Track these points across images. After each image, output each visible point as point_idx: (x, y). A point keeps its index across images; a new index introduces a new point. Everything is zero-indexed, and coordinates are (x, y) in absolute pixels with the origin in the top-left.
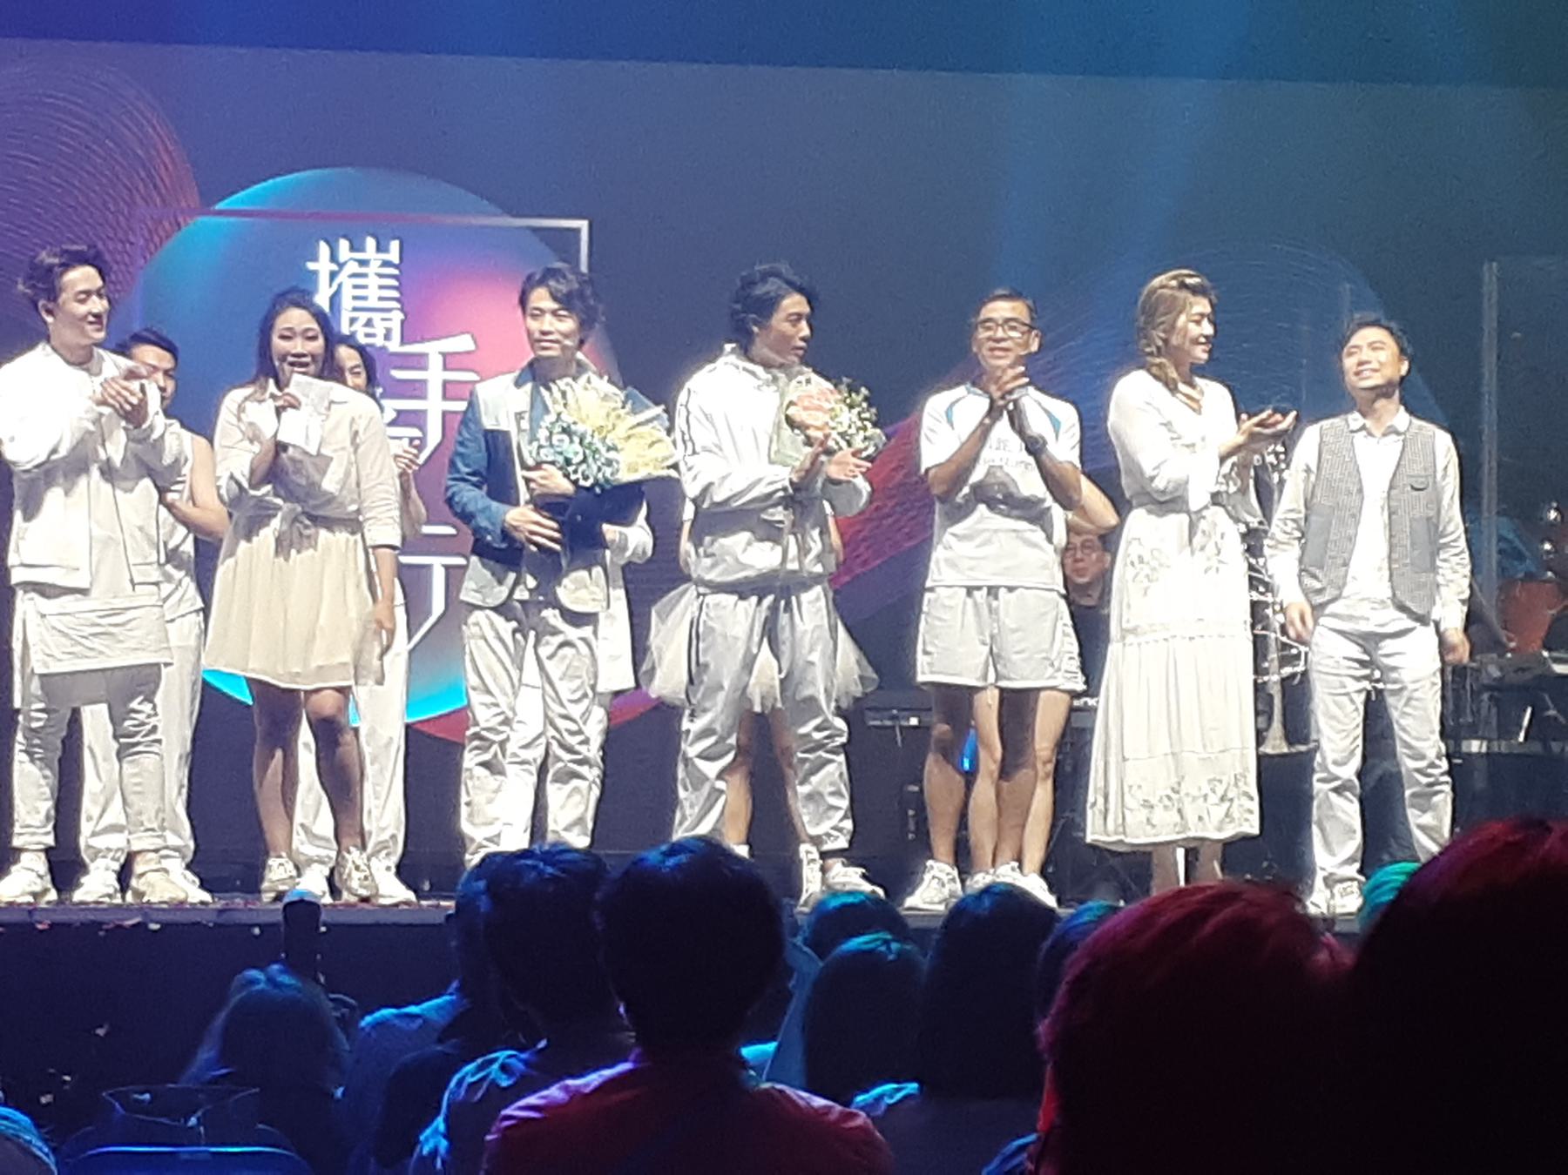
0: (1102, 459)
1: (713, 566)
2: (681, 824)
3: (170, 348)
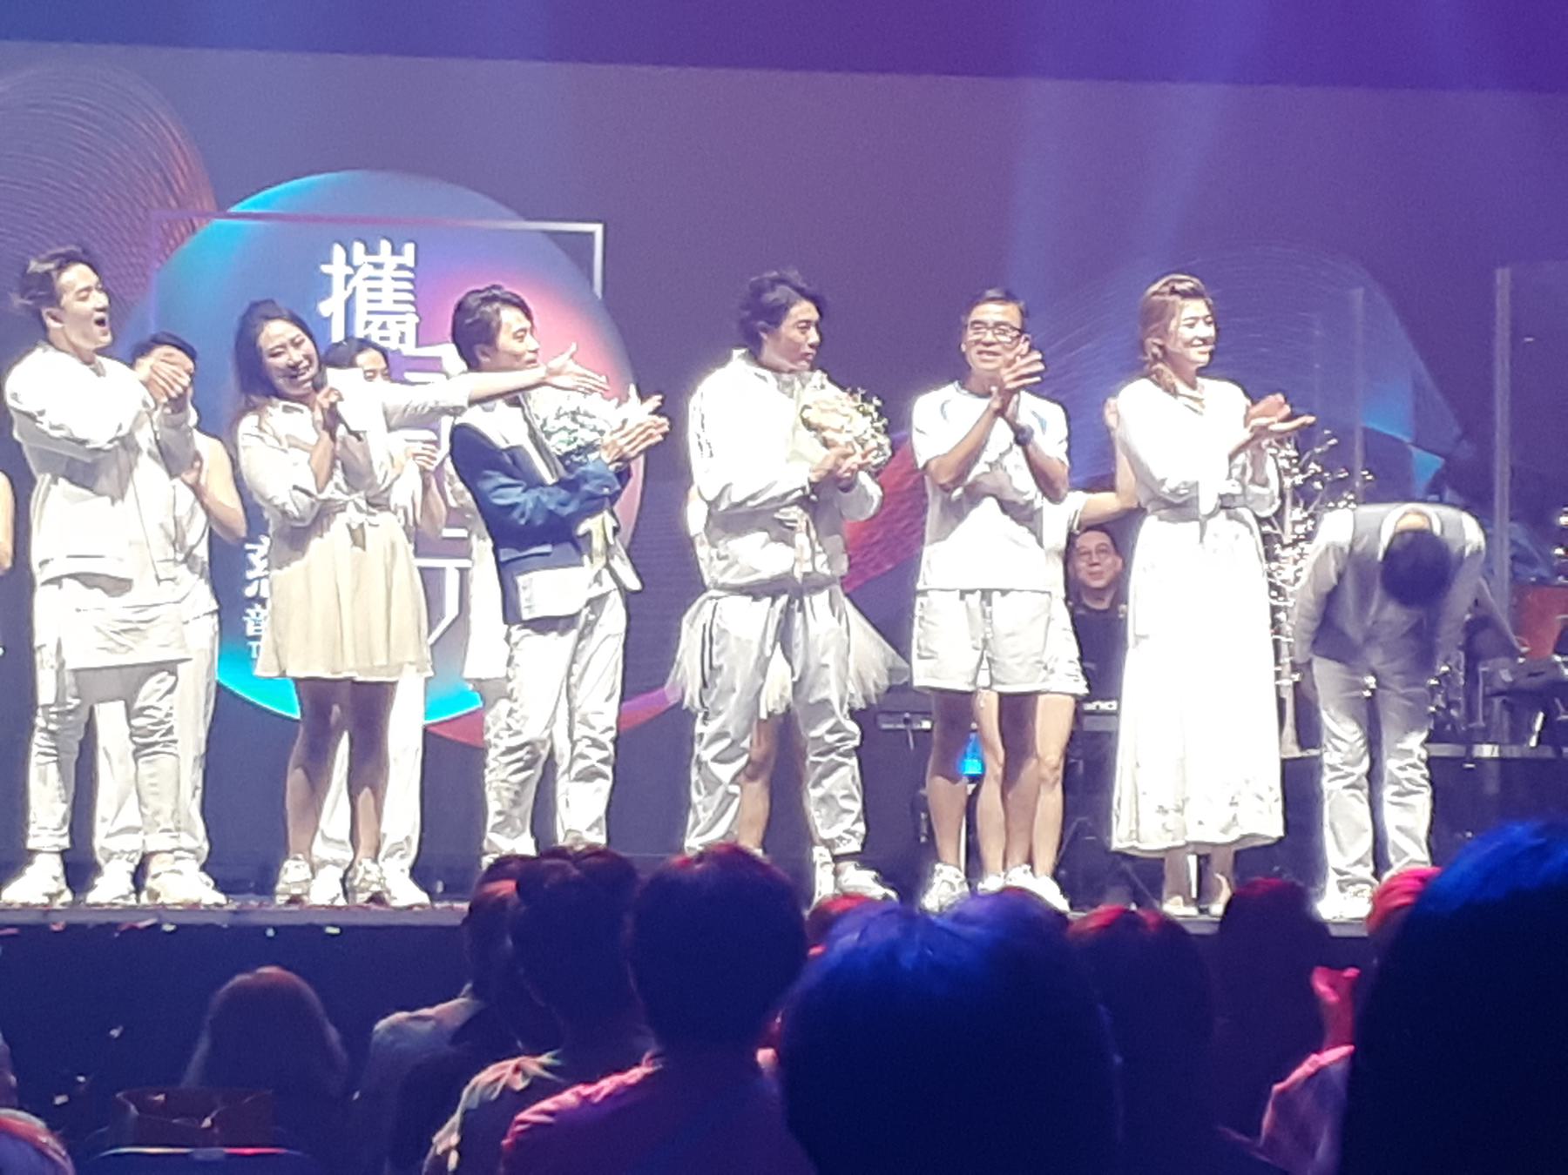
0: (1095, 459)
1: (725, 570)
2: (694, 827)
3: (192, 355)
